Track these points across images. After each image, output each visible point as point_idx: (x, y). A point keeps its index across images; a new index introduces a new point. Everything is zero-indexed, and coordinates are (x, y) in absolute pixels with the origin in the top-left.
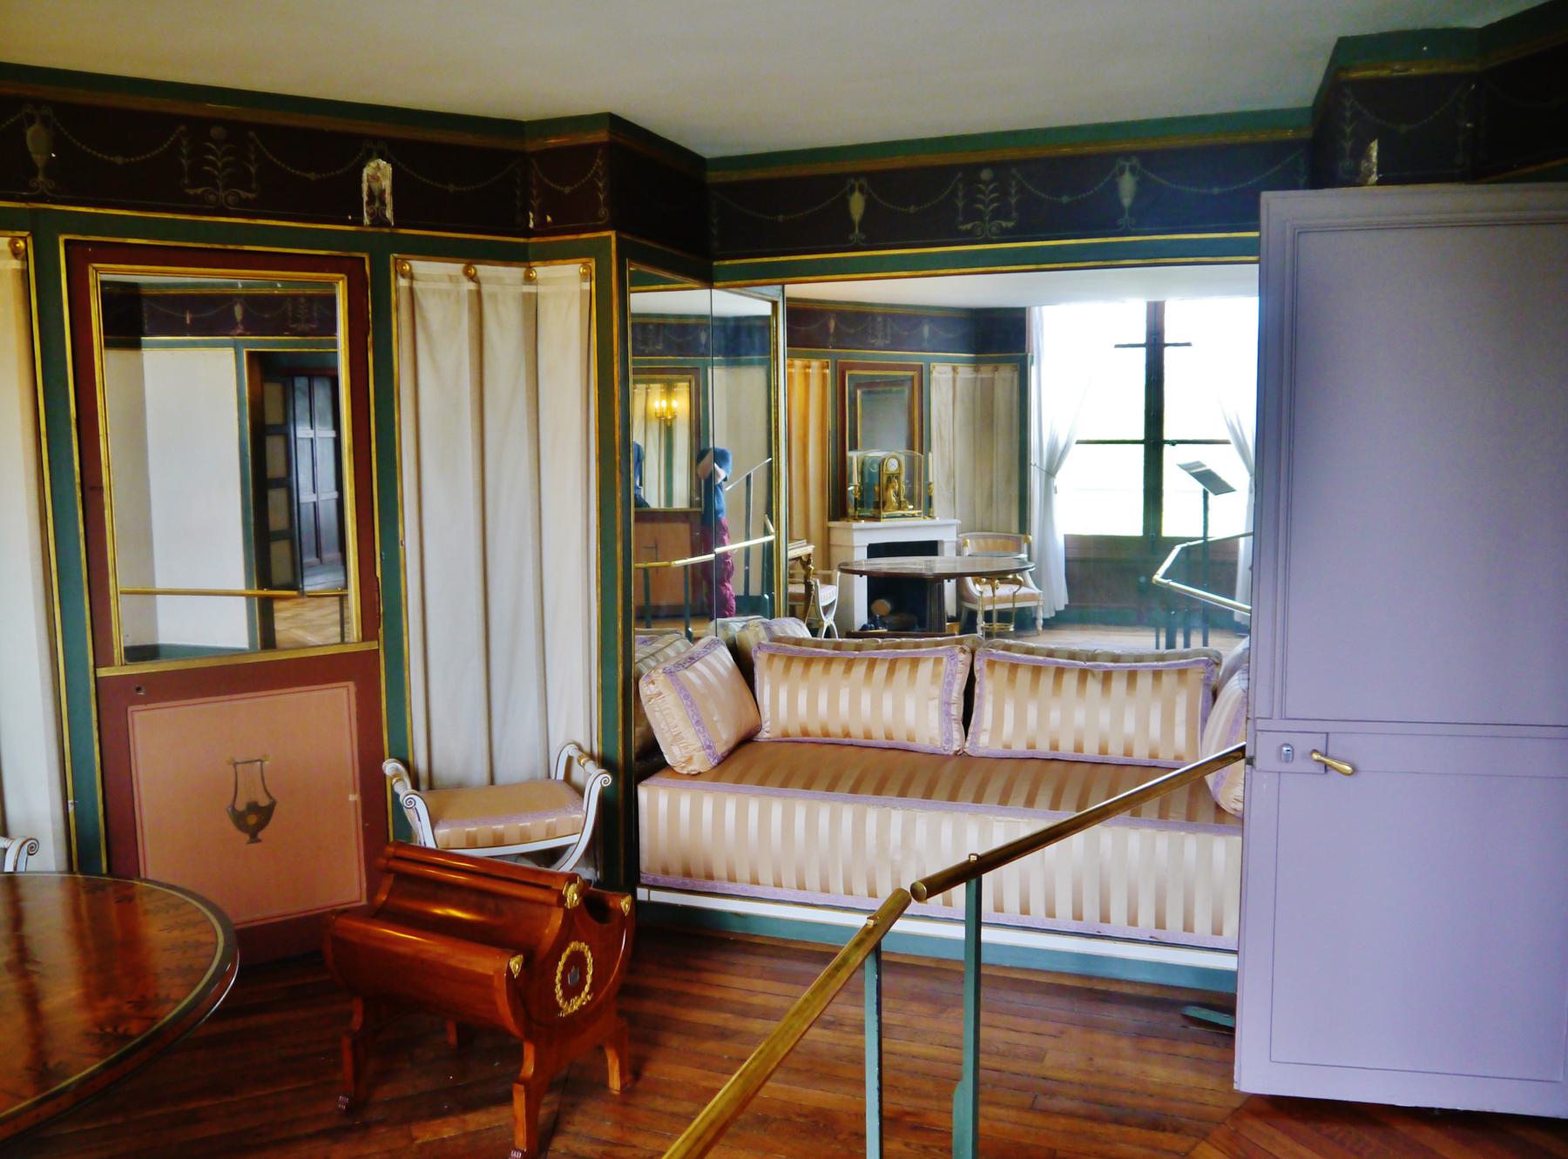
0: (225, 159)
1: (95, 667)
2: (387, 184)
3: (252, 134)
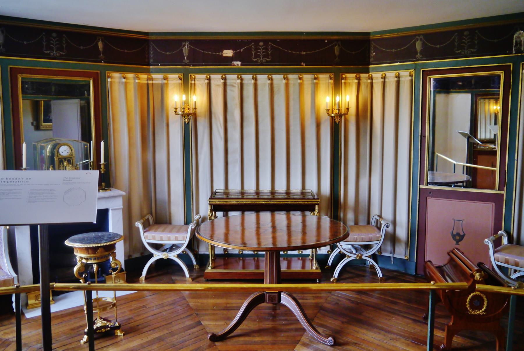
0: (468, 41)
1: (420, 185)
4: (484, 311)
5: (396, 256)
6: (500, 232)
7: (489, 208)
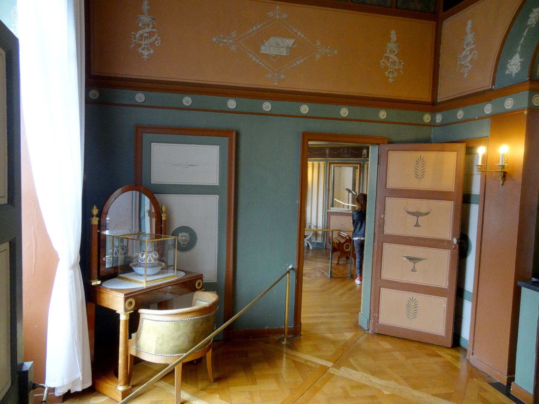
2: (366, 153)
5: (317, 241)
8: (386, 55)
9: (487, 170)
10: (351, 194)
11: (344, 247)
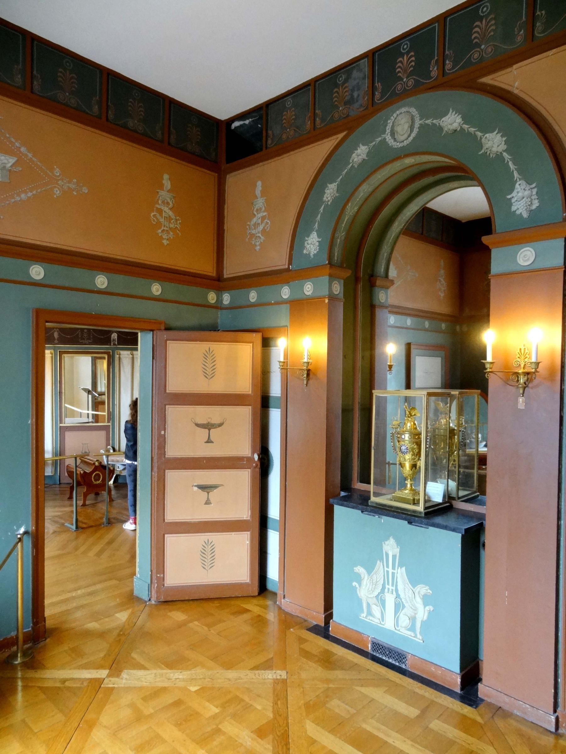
2: (116, 338)
3: (91, 330)
4: (101, 481)
6: (108, 447)
7: (103, 433)
8: (159, 207)
9: (288, 367)
10: (90, 396)
11: (93, 479)
